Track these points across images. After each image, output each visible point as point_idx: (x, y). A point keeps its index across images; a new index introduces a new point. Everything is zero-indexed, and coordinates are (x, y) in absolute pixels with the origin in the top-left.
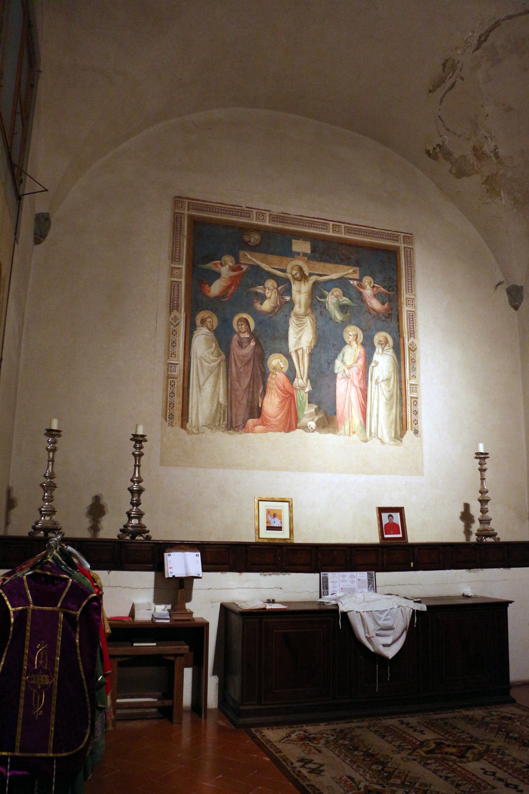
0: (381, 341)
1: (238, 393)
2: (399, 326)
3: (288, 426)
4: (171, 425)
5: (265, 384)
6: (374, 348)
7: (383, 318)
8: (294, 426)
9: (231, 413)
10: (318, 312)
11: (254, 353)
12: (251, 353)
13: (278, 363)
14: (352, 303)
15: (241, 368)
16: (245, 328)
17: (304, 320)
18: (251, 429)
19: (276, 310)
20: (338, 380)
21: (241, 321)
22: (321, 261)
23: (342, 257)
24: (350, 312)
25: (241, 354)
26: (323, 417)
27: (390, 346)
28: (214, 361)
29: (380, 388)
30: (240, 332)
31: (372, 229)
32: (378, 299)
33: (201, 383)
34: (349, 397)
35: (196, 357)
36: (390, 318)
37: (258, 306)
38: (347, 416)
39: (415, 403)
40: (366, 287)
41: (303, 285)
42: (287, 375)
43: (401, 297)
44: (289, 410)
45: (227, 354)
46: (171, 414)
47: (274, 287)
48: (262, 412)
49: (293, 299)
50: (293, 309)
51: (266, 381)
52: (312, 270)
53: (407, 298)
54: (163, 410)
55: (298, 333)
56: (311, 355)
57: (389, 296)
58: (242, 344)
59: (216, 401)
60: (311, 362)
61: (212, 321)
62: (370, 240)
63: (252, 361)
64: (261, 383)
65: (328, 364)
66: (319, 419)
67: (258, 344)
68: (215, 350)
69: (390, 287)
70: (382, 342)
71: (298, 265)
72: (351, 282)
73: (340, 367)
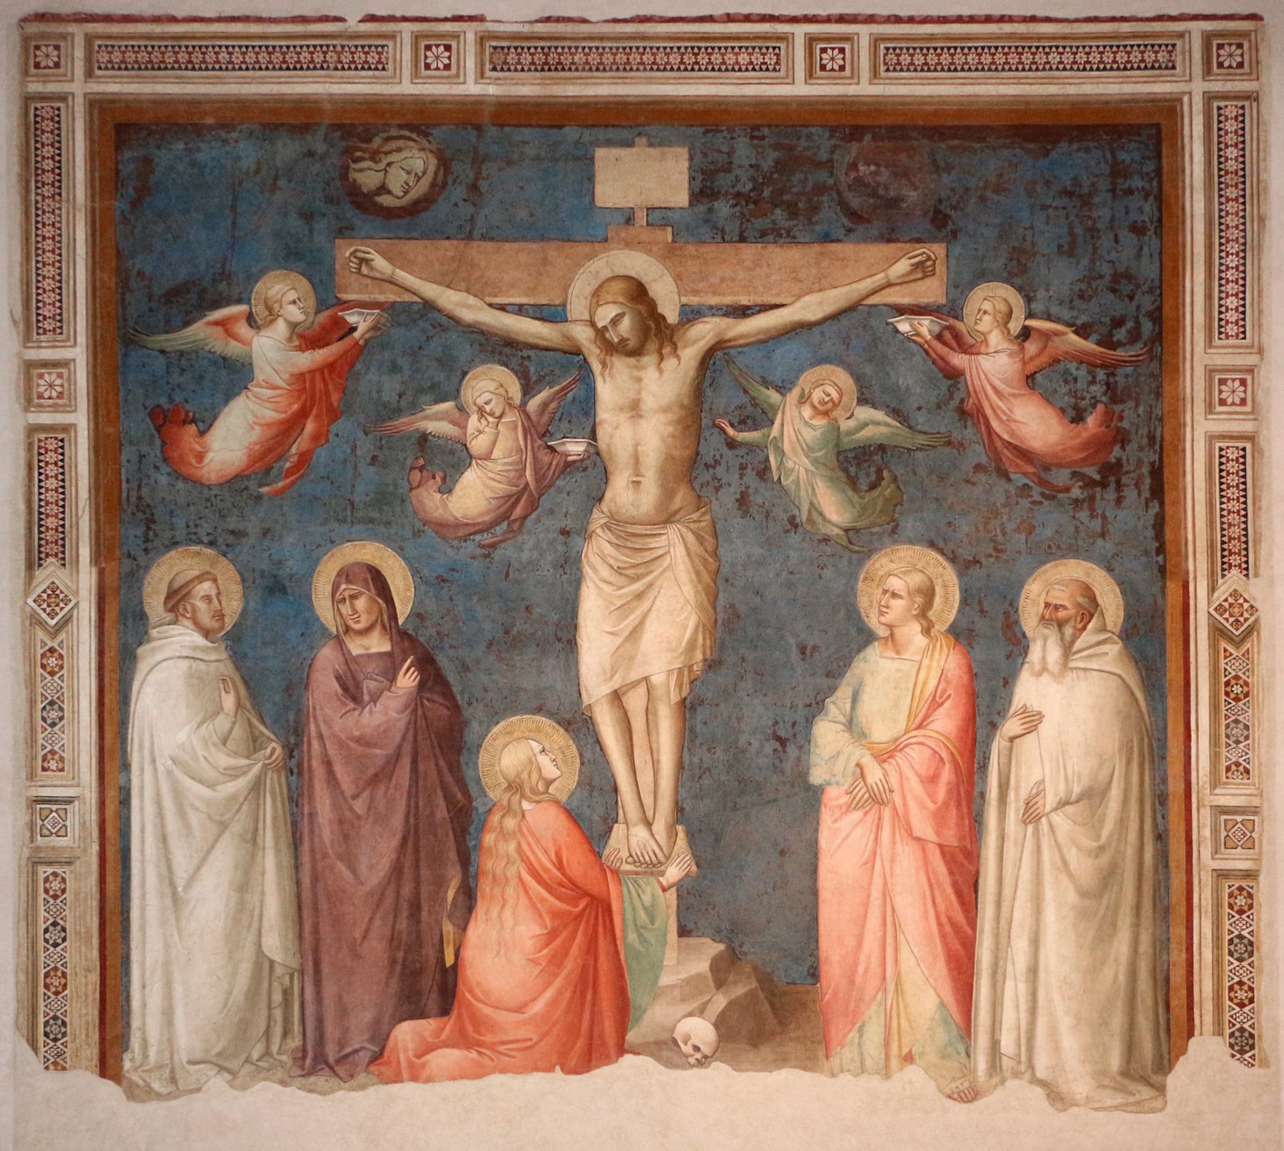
0: (1057, 607)
2: (1159, 525)
3: (580, 1044)
6: (1017, 645)
7: (1076, 492)
10: (728, 497)
11: (413, 724)
12: (401, 725)
13: (531, 762)
14: (905, 431)
15: (355, 797)
16: (369, 612)
17: (653, 543)
18: (411, 1065)
19: (518, 512)
20: (826, 817)
21: (349, 581)
22: (743, 239)
23: (855, 202)
24: (895, 479)
25: (356, 733)
26: (751, 995)
27: (1110, 626)
28: (233, 773)
30: (348, 629)
31: (1021, 28)
32: (1048, 398)
33: (181, 875)
34: (885, 893)
36: (1113, 485)
37: (431, 501)
40: (986, 341)
41: (650, 374)
42: (572, 815)
43: (1176, 370)
44: (584, 968)
45: (292, 740)
47: (508, 402)
48: (461, 986)
49: (603, 442)
50: (600, 499)
51: (479, 846)
52: (696, 292)
53: (1210, 372)
55: (624, 610)
56: (687, 708)
57: (1111, 368)
58: (358, 686)
59: (248, 952)
61: (219, 594)
63: (406, 762)
64: (453, 855)
65: (777, 745)
66: (731, 1004)
68: (234, 723)
69: (1118, 323)
70: (1062, 614)
72: (904, 327)
73: (839, 753)
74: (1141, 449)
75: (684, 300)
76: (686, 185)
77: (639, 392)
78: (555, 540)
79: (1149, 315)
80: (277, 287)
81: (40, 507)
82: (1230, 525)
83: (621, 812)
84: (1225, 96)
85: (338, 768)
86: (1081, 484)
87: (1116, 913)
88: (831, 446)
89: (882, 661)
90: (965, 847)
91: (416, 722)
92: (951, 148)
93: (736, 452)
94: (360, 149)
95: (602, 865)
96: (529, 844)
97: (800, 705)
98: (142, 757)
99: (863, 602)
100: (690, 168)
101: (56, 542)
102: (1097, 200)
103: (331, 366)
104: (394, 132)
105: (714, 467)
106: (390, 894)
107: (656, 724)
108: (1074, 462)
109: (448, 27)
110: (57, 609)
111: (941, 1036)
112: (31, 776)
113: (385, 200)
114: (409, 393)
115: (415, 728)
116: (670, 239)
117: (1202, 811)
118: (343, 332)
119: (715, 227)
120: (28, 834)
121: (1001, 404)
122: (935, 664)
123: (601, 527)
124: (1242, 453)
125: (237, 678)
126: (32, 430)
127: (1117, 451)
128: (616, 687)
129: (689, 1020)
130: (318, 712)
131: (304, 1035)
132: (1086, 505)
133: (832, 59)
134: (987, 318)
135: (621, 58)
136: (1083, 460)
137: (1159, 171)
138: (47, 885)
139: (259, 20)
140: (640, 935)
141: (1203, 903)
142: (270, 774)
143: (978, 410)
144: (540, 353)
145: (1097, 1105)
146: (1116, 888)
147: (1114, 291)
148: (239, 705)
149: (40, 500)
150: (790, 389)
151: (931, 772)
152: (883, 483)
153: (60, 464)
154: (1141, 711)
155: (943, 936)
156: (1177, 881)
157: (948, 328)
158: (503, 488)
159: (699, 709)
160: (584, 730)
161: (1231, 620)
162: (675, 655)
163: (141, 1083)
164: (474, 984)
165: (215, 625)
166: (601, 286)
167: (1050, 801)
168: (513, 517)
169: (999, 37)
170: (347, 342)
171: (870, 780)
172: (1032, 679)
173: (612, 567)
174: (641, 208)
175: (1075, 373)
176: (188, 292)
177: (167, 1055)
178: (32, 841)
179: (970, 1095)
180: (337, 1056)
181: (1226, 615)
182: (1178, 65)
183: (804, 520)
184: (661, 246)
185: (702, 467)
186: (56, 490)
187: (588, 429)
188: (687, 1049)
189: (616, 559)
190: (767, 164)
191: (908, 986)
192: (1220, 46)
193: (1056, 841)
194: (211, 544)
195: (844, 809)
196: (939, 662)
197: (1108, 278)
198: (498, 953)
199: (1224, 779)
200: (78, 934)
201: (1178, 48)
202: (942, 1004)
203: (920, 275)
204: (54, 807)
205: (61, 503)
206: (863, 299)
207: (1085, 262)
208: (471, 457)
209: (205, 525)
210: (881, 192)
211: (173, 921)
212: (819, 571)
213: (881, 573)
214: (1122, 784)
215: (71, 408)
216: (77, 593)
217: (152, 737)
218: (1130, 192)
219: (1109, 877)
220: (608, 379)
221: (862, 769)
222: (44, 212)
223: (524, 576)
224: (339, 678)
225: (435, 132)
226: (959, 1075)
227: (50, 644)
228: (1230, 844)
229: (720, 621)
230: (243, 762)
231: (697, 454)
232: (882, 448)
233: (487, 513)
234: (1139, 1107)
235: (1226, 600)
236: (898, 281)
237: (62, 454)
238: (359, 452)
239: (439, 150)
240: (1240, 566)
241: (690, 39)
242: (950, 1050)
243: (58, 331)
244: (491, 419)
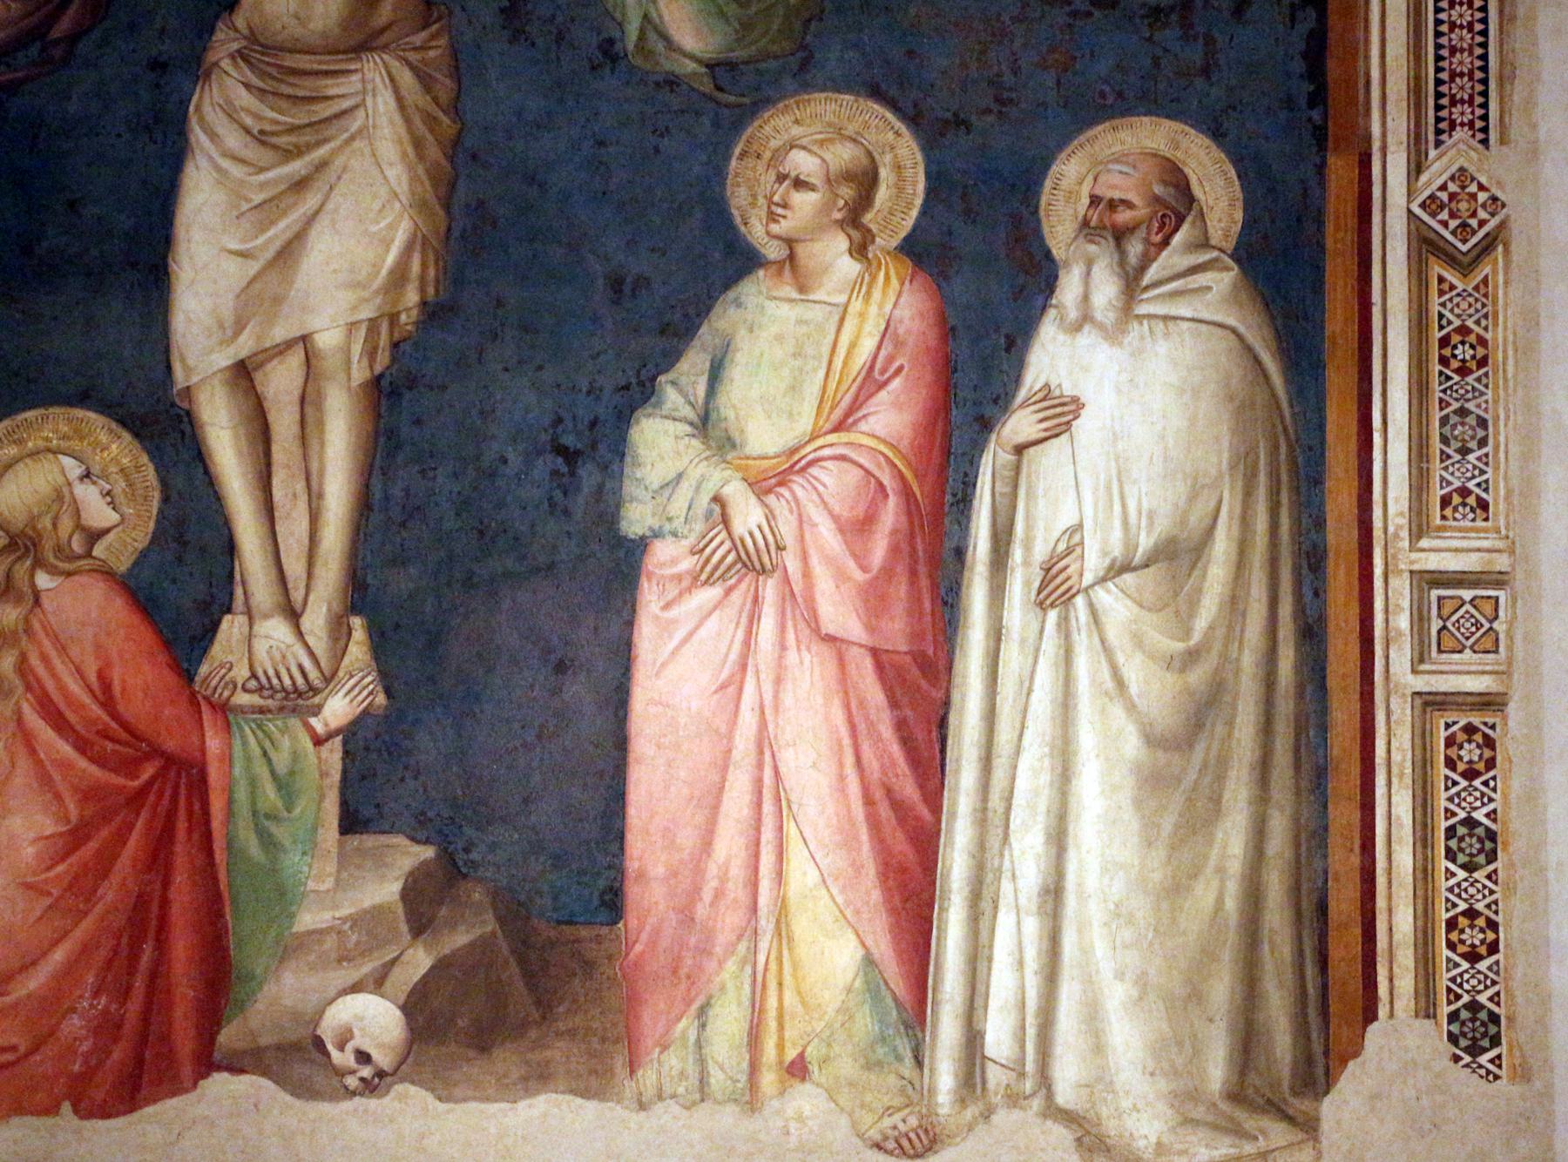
8: (185, 1043)
20: (650, 599)
26: (483, 945)
29: (1083, 643)
34: (763, 743)
38: (730, 920)
39: (1470, 752)
60: (390, 455)
83: (239, 591)
87: (1220, 778)
90: (923, 654)
97: (608, 389)
107: (321, 424)
117: (1394, 582)
128: (243, 354)
141: (1396, 757)
146: (1220, 730)
151: (860, 511)
156: (1343, 713)
167: (1093, 563)
171: (739, 528)
172: (1061, 337)
191: (801, 925)
193: (1103, 642)
195: (685, 583)
196: (881, 307)
199: (1438, 522)
214: (1236, 532)
221: (723, 506)
228: (1448, 643)
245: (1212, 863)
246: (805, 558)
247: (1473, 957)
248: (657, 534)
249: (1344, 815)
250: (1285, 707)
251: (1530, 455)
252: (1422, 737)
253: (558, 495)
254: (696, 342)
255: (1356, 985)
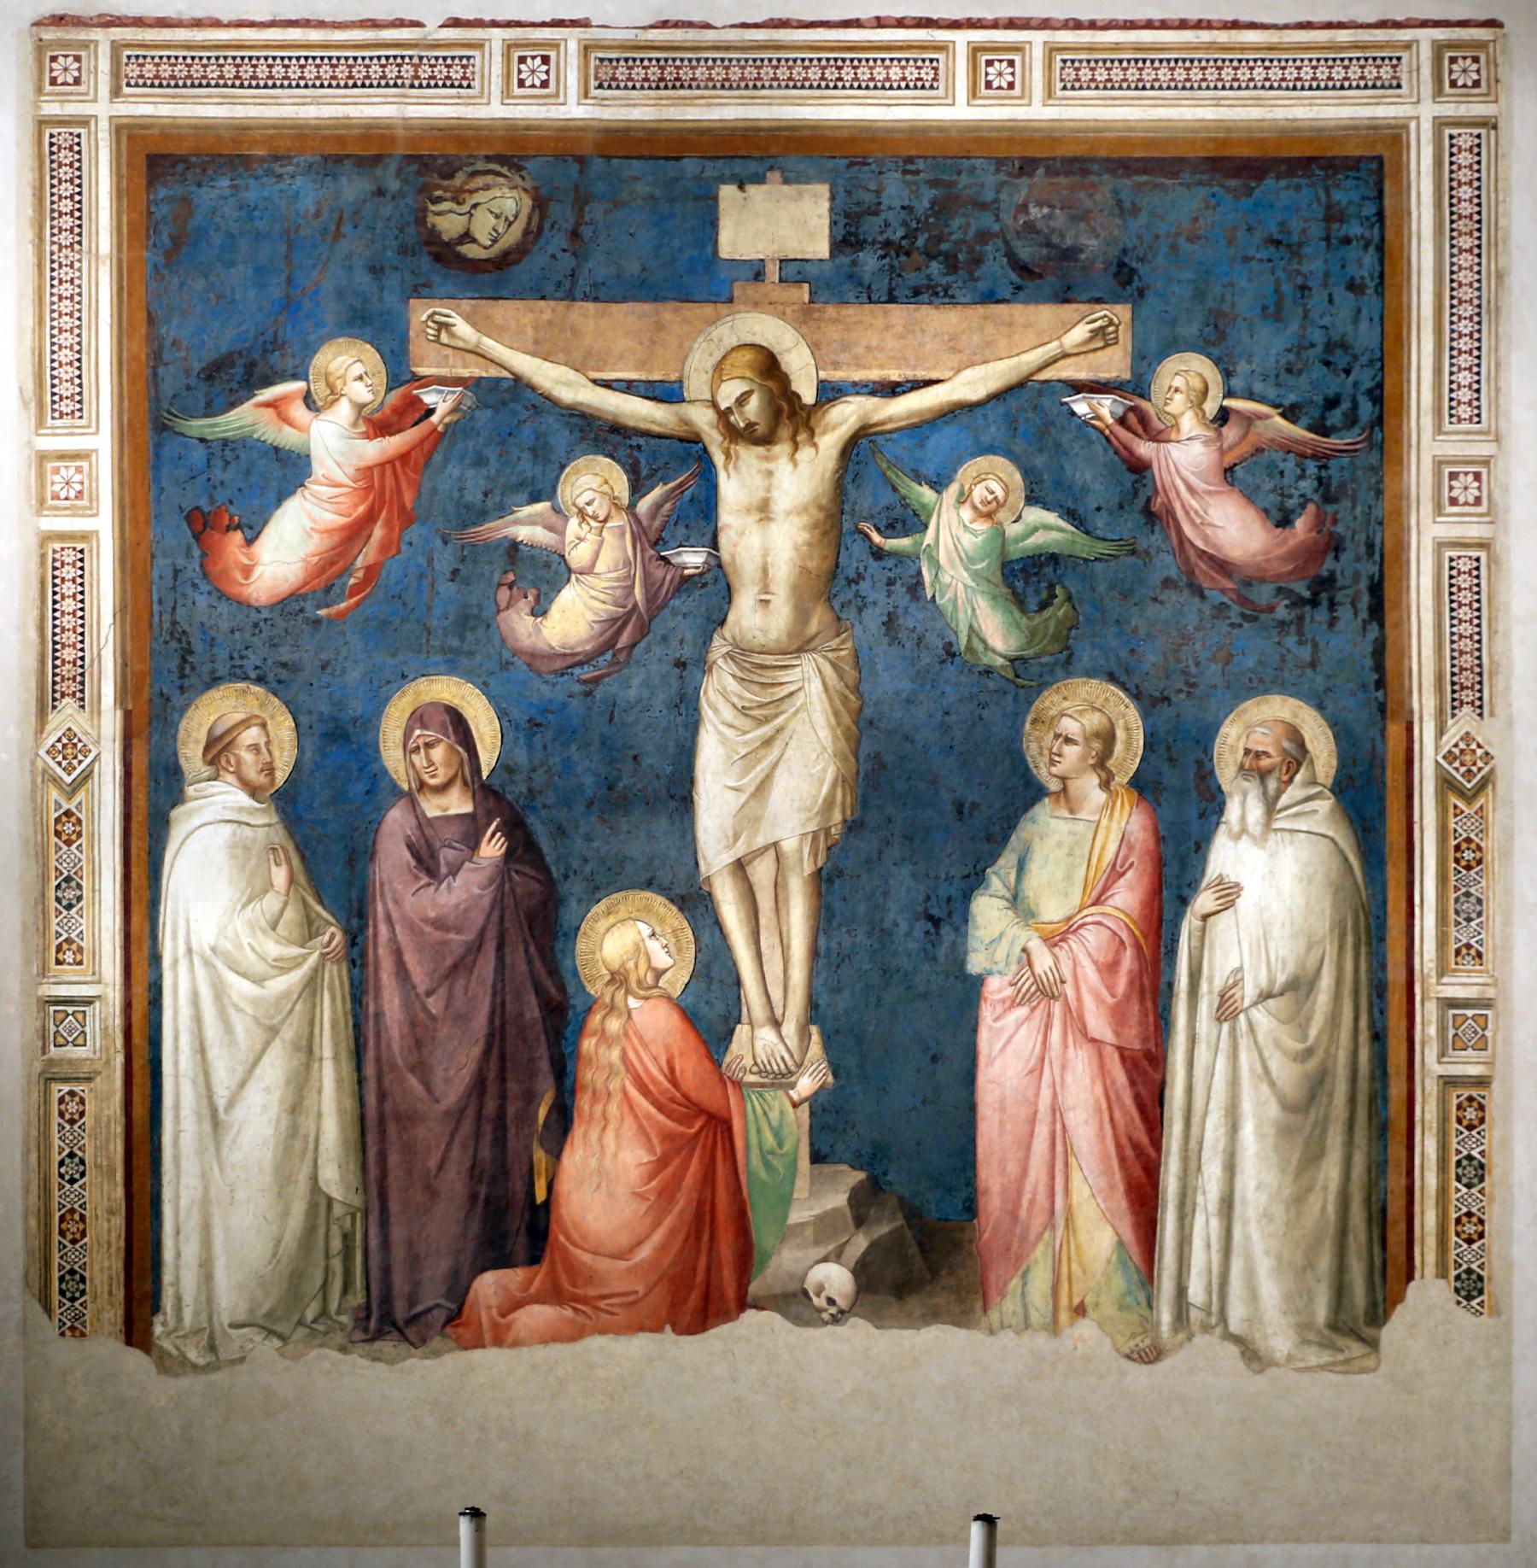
0: (1258, 755)
1: (420, 1132)
2: (1379, 651)
3: (694, 1299)
4: (73, 1328)
5: (564, 1070)
6: (1212, 803)
7: (1282, 612)
9: (386, 1243)
10: (873, 619)
11: (499, 902)
12: (486, 902)
13: (639, 949)
14: (1081, 538)
15: (429, 993)
16: (447, 764)
17: (783, 676)
18: (495, 1326)
20: (987, 1013)
21: (424, 726)
22: (892, 299)
23: (1025, 252)
24: (1069, 598)
25: (432, 914)
26: (895, 1237)
27: (1321, 778)
28: (283, 966)
29: (1244, 1043)
30: (422, 785)
31: (1222, 37)
32: (1250, 496)
33: (222, 1094)
35: (190, 951)
36: (1325, 603)
37: (520, 625)
41: (783, 467)
42: (689, 1015)
43: (1400, 462)
44: (700, 1203)
45: (355, 922)
46: (72, 1272)
47: (614, 502)
48: (554, 1227)
49: (725, 554)
50: (722, 623)
51: (576, 1054)
52: (836, 365)
53: (1439, 463)
54: (29, 1252)
55: (749, 759)
56: (824, 882)
57: (1323, 458)
58: (433, 855)
59: (301, 1188)
60: (829, 920)
61: (268, 743)
62: (1209, 113)
64: (544, 1065)
66: (873, 1246)
67: (522, 847)
68: (286, 904)
69: (1332, 403)
70: (1265, 763)
71: (753, 346)
72: (1081, 407)
73: (1001, 935)
74: (1358, 559)
75: (823, 375)
76: (827, 231)
77: (768, 489)
78: (668, 673)
79: (1369, 392)
80: (340, 359)
81: (54, 634)
82: (1461, 653)
83: (744, 1010)
84: (1457, 123)
85: (410, 958)
86: (1287, 602)
87: (1324, 1131)
88: (994, 556)
89: (1053, 821)
91: (502, 900)
92: (1140, 185)
93: (883, 563)
94: (438, 187)
95: (721, 1075)
96: (637, 1054)
98: (175, 948)
99: (1031, 749)
100: (831, 210)
101: (74, 679)
102: (1307, 250)
103: (404, 457)
104: (480, 166)
105: (857, 583)
106: (471, 1112)
107: (787, 900)
108: (1279, 576)
109: (546, 33)
110: (75, 762)
111: (1119, 1283)
112: (44, 971)
113: (470, 251)
114: (497, 491)
115: (502, 909)
116: (806, 298)
117: (1427, 1005)
118: (417, 416)
119: (860, 284)
120: (40, 1044)
121: (1193, 502)
122: (1114, 825)
123: (724, 656)
124: (1475, 564)
125: (290, 847)
126: (47, 537)
127: (1329, 564)
129: (822, 1266)
130: (386, 888)
131: (368, 1288)
132: (1293, 629)
133: (1000, 74)
134: (1178, 396)
135: (751, 72)
136: (1291, 573)
137: (1380, 215)
138: (63, 1107)
139: (321, 24)
140: (767, 1165)
141: (1428, 1116)
142: (328, 965)
143: (1167, 511)
144: (652, 441)
145: (1302, 1365)
146: (1324, 1100)
147: (1327, 364)
148: (292, 880)
149: (55, 626)
150: (947, 486)
151: (1110, 957)
152: (1056, 601)
153: (79, 581)
154: (1356, 883)
155: (1122, 1160)
156: (1397, 1089)
157: (1132, 409)
158: (607, 609)
159: (837, 882)
160: (701, 909)
161: (1463, 769)
162: (811, 814)
163: (175, 1352)
164: (569, 1224)
165: (262, 779)
166: (724, 358)
167: (1249, 992)
168: (619, 645)
169: (1196, 48)
170: (422, 428)
171: (1038, 970)
172: (1230, 844)
173: (734, 705)
174: (773, 260)
175: (1282, 465)
176: (233, 365)
177: (204, 1317)
178: (44, 1053)
179: (1151, 1355)
180: (407, 1315)
181: (1457, 764)
182: (1404, 83)
183: (963, 648)
184: (796, 307)
185: (843, 583)
186: (74, 613)
187: (709, 536)
188: (819, 1302)
189: (741, 697)
190: (922, 206)
192: (1453, 60)
193: (1256, 1042)
194: (260, 680)
197: (1320, 348)
198: (598, 1186)
200: (98, 1166)
201: (1404, 61)
202: (1121, 1244)
203: (1101, 344)
204: (70, 1010)
205: (80, 630)
206: (1032, 374)
207: (1294, 326)
208: (570, 571)
209: (252, 657)
210: (1055, 240)
211: (212, 1151)
212: (979, 711)
213: (1052, 713)
214: (1334, 973)
215: (92, 511)
216: (97, 742)
217: (188, 921)
218: (1347, 241)
219: (1317, 1086)
220: (732, 473)
221: (1029, 955)
222: (60, 266)
223: (631, 719)
224: (410, 847)
225: (529, 165)
226: (1140, 1330)
227: (66, 806)
228: (1459, 1044)
229: (862, 775)
230: (296, 951)
231: (837, 566)
232: (1054, 558)
233: (587, 641)
234: (1347, 1367)
235: (1456, 745)
236: (1075, 351)
237: (82, 568)
238: (437, 566)
239: (536, 189)
240: (1472, 703)
241: (832, 49)
242: (1129, 1300)
243: (78, 414)
244: (593, 523)
245: (1320, 1183)
246: (1077, 989)
247: (1470, 1241)
248: (990, 973)
249: (1396, 1151)
250: (1363, 1086)
251: (1507, 922)
252: (1443, 1102)
253: (929, 946)
254: (1009, 847)
255: (1402, 1257)
